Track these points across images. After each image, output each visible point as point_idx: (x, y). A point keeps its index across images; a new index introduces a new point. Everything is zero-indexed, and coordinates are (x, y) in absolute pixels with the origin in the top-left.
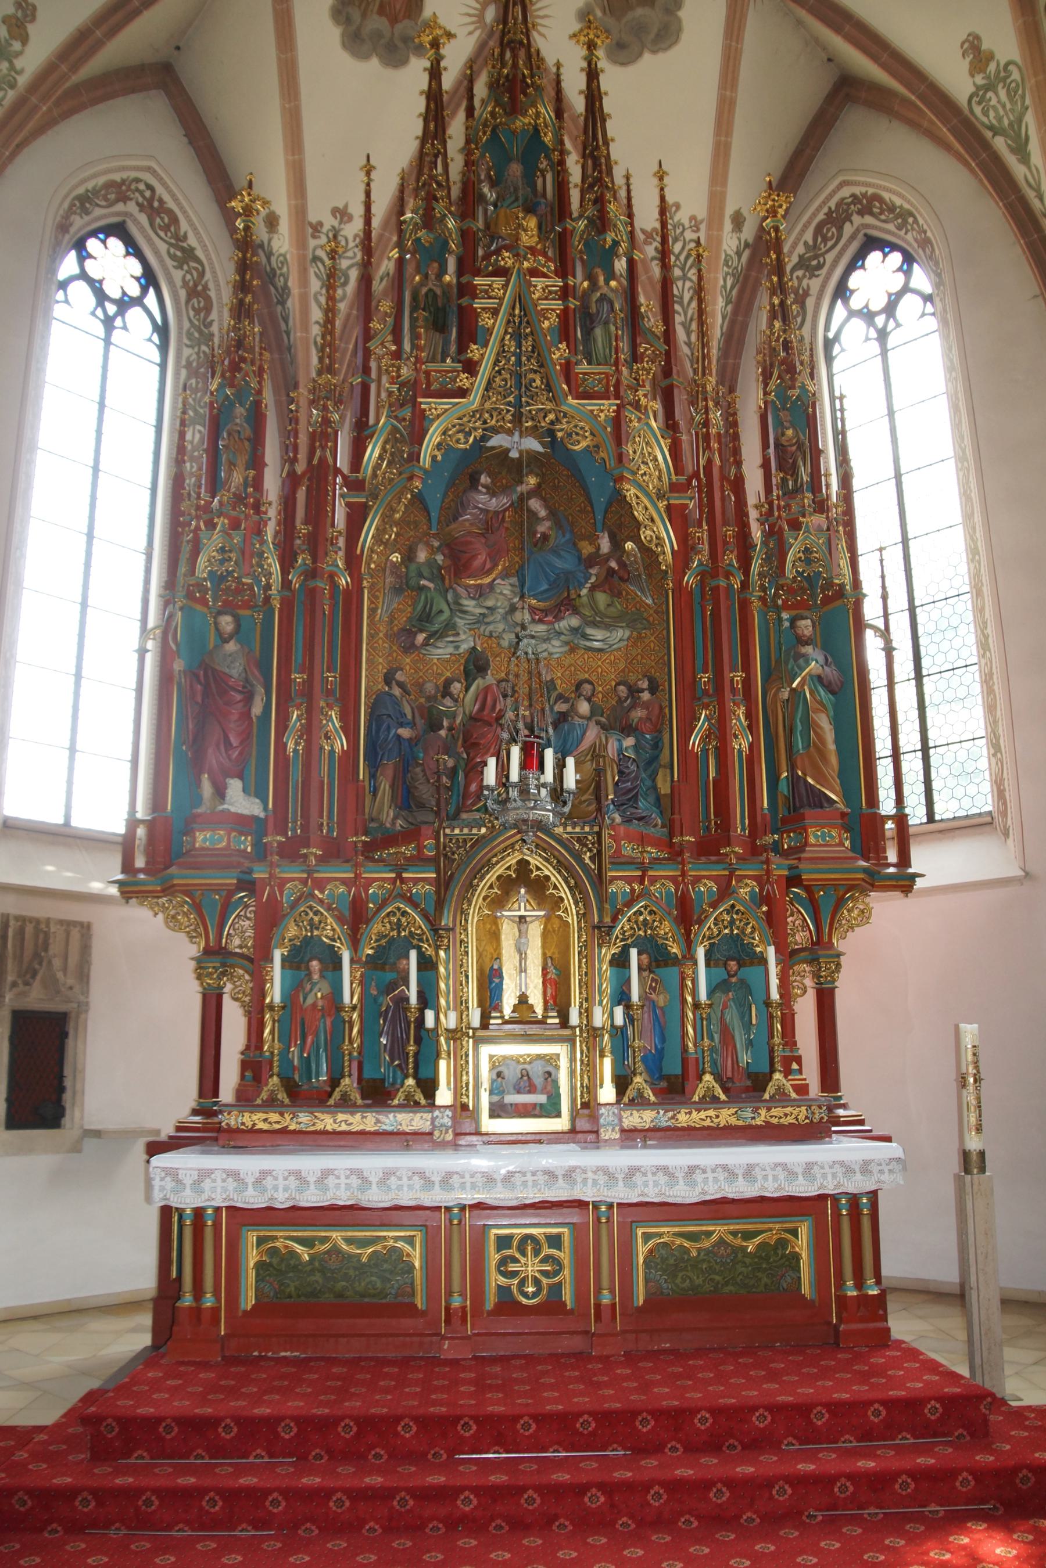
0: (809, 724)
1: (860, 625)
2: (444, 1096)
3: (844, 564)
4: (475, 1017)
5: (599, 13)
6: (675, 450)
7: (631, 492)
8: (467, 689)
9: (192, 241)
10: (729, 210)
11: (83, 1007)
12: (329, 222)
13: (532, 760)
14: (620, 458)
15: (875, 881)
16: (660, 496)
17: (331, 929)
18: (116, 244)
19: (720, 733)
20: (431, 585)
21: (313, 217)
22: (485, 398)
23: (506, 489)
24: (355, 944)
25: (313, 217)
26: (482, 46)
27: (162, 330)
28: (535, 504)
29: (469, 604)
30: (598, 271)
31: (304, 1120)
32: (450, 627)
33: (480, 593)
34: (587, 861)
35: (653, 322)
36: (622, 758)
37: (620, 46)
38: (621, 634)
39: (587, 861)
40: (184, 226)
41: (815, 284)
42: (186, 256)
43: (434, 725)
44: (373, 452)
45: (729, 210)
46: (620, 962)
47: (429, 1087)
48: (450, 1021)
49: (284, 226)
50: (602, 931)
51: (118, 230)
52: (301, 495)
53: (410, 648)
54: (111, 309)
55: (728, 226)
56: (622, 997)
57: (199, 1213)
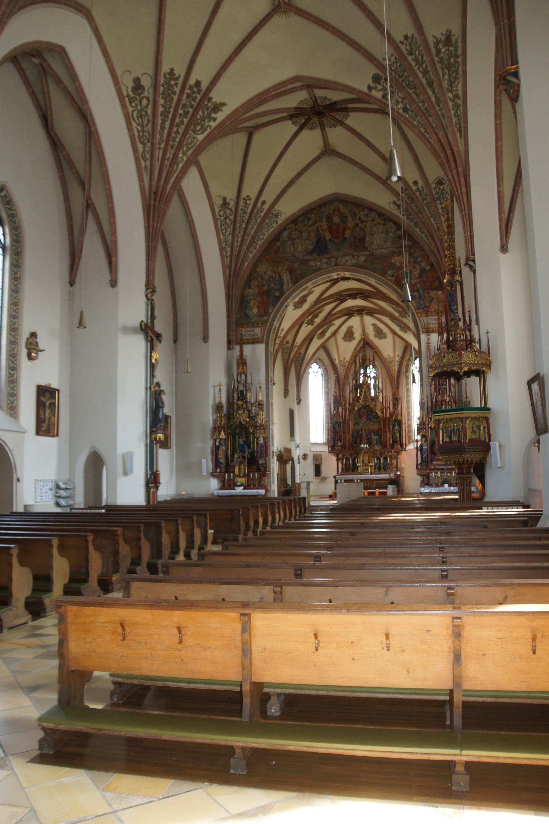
1: (402, 423)
2: (359, 471)
4: (362, 464)
7: (377, 411)
9: (325, 363)
11: (321, 463)
14: (375, 408)
15: (402, 450)
16: (381, 410)
17: (349, 457)
18: (315, 364)
19: (386, 436)
21: (341, 359)
24: (351, 458)
27: (322, 374)
29: (362, 421)
31: (347, 473)
33: (363, 420)
35: (381, 388)
36: (376, 439)
38: (377, 424)
40: (324, 361)
41: (410, 363)
42: (324, 365)
43: (358, 436)
44: (350, 407)
45: (397, 354)
46: (374, 459)
47: (358, 470)
48: (359, 465)
50: (372, 457)
51: (316, 362)
52: (344, 410)
54: (315, 374)
55: (397, 357)
56: (375, 462)
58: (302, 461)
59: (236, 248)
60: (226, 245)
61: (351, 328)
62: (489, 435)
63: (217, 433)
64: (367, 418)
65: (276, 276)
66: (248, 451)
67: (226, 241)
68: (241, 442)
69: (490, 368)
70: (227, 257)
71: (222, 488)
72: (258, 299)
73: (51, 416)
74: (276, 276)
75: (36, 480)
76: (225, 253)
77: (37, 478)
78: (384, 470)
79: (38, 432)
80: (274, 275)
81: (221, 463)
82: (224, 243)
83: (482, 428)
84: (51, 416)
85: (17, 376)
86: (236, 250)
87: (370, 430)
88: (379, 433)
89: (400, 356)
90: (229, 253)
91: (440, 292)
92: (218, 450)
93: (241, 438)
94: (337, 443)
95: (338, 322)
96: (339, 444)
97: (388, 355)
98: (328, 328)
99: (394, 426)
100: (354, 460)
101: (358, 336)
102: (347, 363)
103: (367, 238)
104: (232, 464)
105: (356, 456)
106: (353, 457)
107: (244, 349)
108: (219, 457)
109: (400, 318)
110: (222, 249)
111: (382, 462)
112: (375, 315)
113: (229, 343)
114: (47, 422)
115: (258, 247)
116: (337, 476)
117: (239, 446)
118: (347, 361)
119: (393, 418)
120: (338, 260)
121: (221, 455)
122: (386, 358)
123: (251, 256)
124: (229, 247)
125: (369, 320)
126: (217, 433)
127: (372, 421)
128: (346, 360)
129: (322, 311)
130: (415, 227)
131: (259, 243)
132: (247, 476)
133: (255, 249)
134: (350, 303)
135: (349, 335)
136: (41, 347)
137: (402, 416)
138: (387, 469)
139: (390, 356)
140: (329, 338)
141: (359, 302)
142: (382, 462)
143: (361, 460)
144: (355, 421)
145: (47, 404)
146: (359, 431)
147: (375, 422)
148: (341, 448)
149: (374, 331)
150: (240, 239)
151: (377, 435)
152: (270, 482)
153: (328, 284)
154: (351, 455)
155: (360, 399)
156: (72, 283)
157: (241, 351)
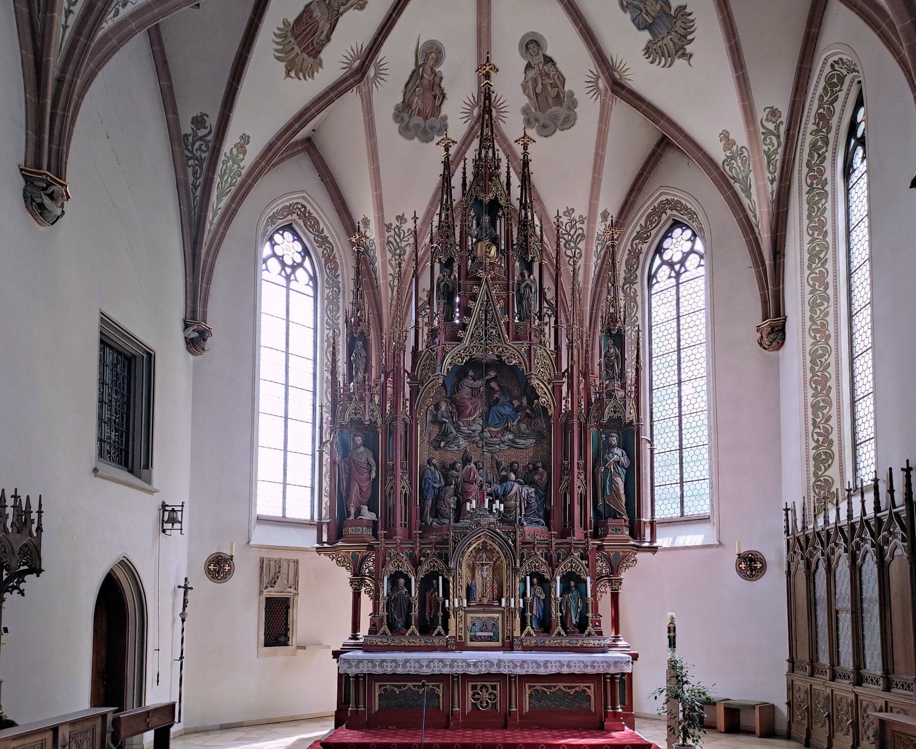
0: (612, 481)
5: (533, 110)
8: (463, 469)
20: (447, 421)
22: (471, 342)
23: (481, 377)
30: (525, 271)
34: (510, 543)
37: (544, 127)
39: (510, 543)
53: (438, 448)
64: (486, 417)
88: (536, 477)
94: (358, 512)
96: (368, 515)
99: (604, 448)
105: (440, 564)
106: (424, 569)
119: (608, 413)
127: (507, 429)
144: (436, 430)
146: (453, 466)
147: (519, 434)
148: (375, 534)
149: (524, 87)
154: (416, 563)
155: (464, 327)
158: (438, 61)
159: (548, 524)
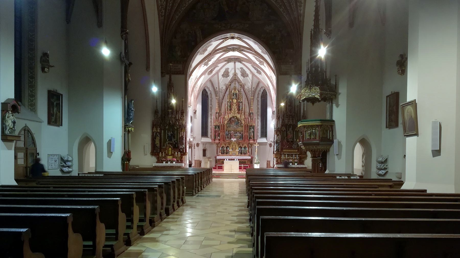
2: (230, 154)
3: (254, 124)
6: (244, 116)
10: (253, 87)
12: (221, 88)
13: (234, 139)
25: (220, 88)
26: (233, 76)
28: (236, 119)
32: (230, 127)
40: (210, 89)
45: (253, 87)
49: (218, 88)
56: (239, 149)
57: (219, 159)
58: (196, 147)
59: (168, 11)
60: (162, 8)
61: (228, 69)
62: (333, 136)
63: (155, 128)
65: (192, 33)
66: (174, 140)
67: (162, 5)
68: (170, 135)
69: (336, 97)
70: (162, 16)
71: (157, 162)
72: (181, 46)
73: (58, 112)
74: (192, 33)
75: (48, 154)
76: (161, 13)
77: (48, 154)
78: (244, 154)
79: (49, 123)
80: (191, 32)
81: (157, 147)
82: (161, 7)
83: (329, 131)
84: (58, 112)
85: (35, 83)
86: (168, 13)
87: (236, 131)
89: (255, 88)
90: (163, 14)
91: (292, 50)
92: (156, 139)
93: (169, 132)
95: (220, 65)
97: (248, 87)
98: (214, 68)
100: (227, 148)
101: (231, 75)
102: (224, 91)
103: (250, 12)
104: (164, 147)
105: (228, 145)
107: (172, 77)
108: (156, 143)
109: (260, 65)
110: (159, 11)
111: (243, 149)
112: (243, 62)
113: (162, 73)
114: (55, 116)
115: (181, 11)
116: (217, 157)
117: (168, 137)
118: (224, 89)
120: (232, 26)
121: (157, 142)
122: (247, 89)
123: (177, 17)
124: (163, 10)
125: (239, 65)
126: (155, 128)
128: (223, 89)
129: (214, 57)
130: (280, 8)
131: (183, 8)
132: (173, 155)
133: (180, 13)
134: (231, 54)
135: (226, 74)
136: (51, 63)
137: (255, 124)
138: (246, 153)
139: (249, 88)
140: (214, 75)
141: (236, 54)
142: (243, 149)
143: (231, 148)
145: (55, 103)
150: (171, 5)
151: (241, 134)
152: (187, 159)
153: (222, 40)
154: (225, 145)
156: (68, 20)
157: (170, 79)
158: (228, 69)
159: (243, 139)
